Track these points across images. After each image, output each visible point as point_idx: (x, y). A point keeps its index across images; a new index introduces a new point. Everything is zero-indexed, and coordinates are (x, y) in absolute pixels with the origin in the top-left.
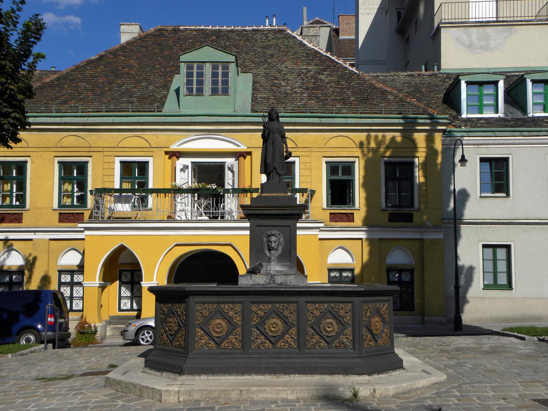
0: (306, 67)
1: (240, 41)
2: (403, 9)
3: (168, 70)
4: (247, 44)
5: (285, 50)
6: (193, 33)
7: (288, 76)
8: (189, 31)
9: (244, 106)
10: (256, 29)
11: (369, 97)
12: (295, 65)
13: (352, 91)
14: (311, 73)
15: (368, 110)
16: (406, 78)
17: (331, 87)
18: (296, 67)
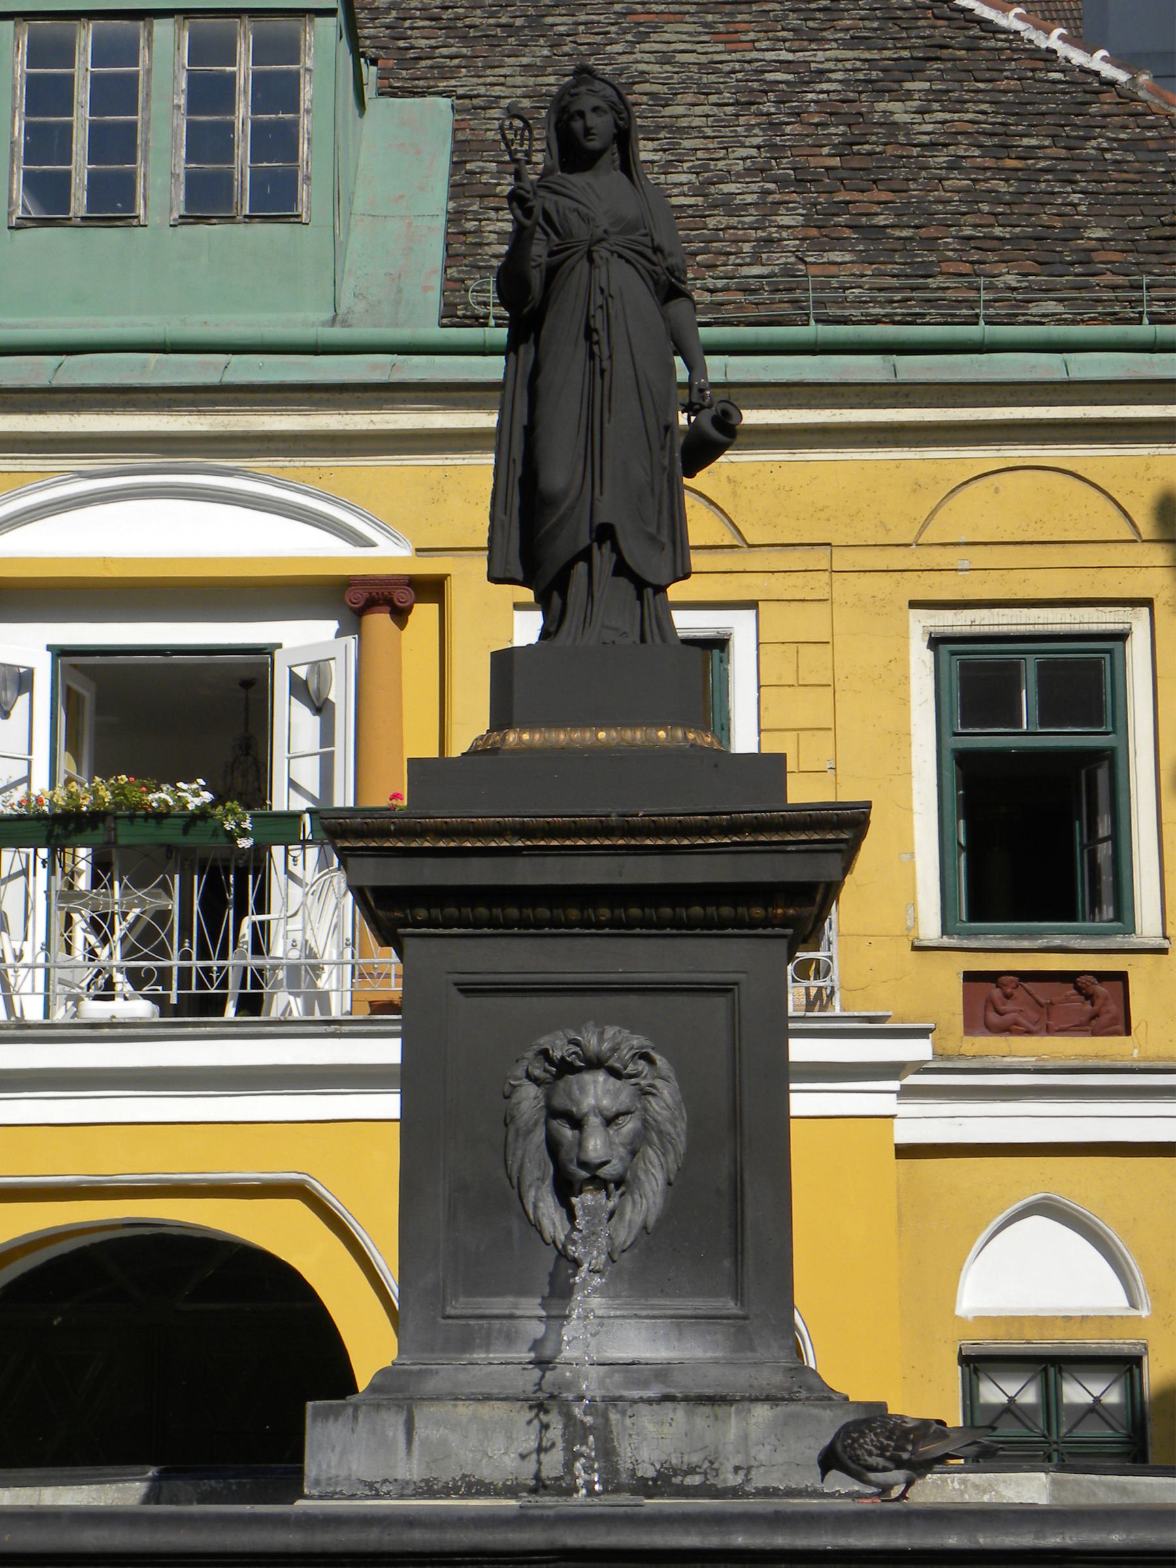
0: (790, 57)
7: (680, 110)
9: (400, 291)
12: (721, 47)
13: (1092, 187)
14: (825, 86)
17: (954, 165)
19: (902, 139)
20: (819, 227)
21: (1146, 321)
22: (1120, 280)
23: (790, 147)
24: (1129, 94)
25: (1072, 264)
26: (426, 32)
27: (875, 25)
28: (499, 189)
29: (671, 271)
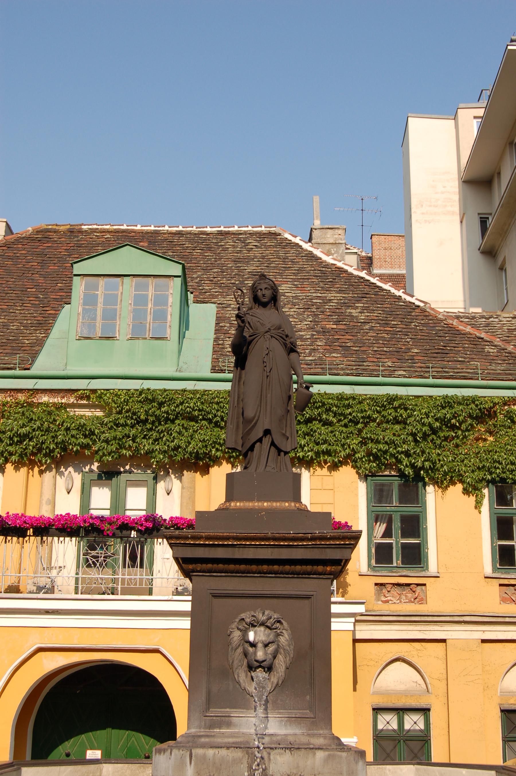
0: (320, 295)
1: (194, 250)
2: (491, 214)
3: (52, 297)
4: (206, 254)
5: (280, 266)
6: (106, 237)
7: (287, 310)
8: (98, 233)
10: (225, 231)
11: (449, 348)
12: (299, 292)
13: (413, 337)
14: (332, 304)
15: (447, 372)
16: (513, 322)
17: (372, 328)
18: (301, 295)
19: (355, 320)
20: (330, 346)
21: (431, 378)
22: (423, 365)
23: (321, 322)
24: (423, 310)
25: (408, 360)
26: (208, 285)
27: (346, 287)
28: (230, 331)
29: (292, 343)
